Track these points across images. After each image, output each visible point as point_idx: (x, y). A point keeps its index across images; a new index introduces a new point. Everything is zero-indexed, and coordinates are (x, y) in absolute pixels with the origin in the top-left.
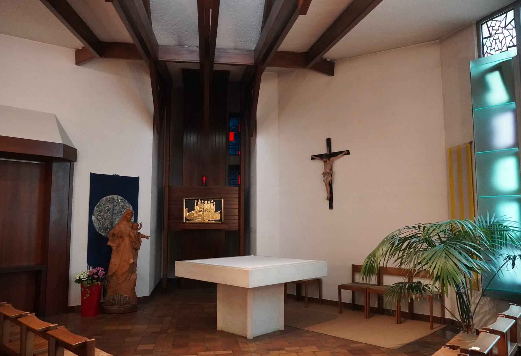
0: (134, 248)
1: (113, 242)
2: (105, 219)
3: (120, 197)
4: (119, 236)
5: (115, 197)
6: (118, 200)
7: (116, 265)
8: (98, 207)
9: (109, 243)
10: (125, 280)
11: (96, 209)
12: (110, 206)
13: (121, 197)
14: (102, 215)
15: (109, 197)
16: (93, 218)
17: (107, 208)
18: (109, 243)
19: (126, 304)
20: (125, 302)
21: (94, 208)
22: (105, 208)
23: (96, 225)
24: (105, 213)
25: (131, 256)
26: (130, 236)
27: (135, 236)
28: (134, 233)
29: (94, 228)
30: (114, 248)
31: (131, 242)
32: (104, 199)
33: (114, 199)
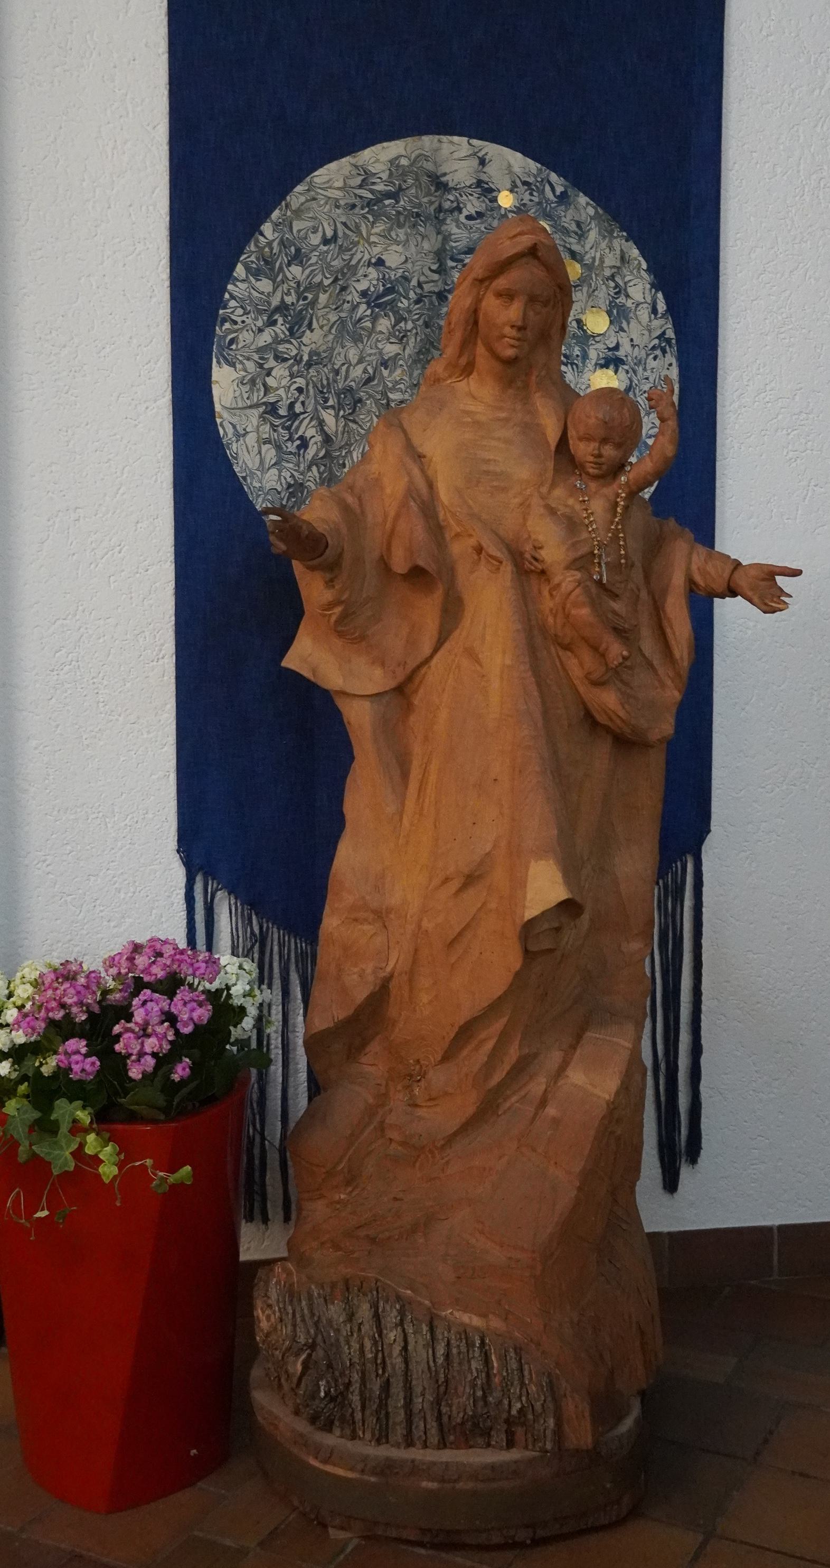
0: (591, 722)
1: (349, 628)
2: (350, 401)
3: (508, 162)
4: (400, 564)
5: (455, 155)
6: (487, 191)
7: (381, 916)
8: (267, 268)
9: (308, 654)
10: (488, 1109)
11: (243, 286)
12: (393, 259)
13: (518, 162)
14: (315, 360)
15: (380, 157)
16: (225, 383)
17: (368, 280)
18: (308, 654)
19: (474, 1431)
20: (461, 1404)
21: (228, 276)
22: (342, 279)
23: (258, 466)
24: (349, 331)
25: (539, 821)
26: (527, 570)
27: (583, 562)
28: (572, 525)
29: (232, 487)
30: (359, 717)
31: (540, 641)
32: (332, 175)
33: (439, 184)
